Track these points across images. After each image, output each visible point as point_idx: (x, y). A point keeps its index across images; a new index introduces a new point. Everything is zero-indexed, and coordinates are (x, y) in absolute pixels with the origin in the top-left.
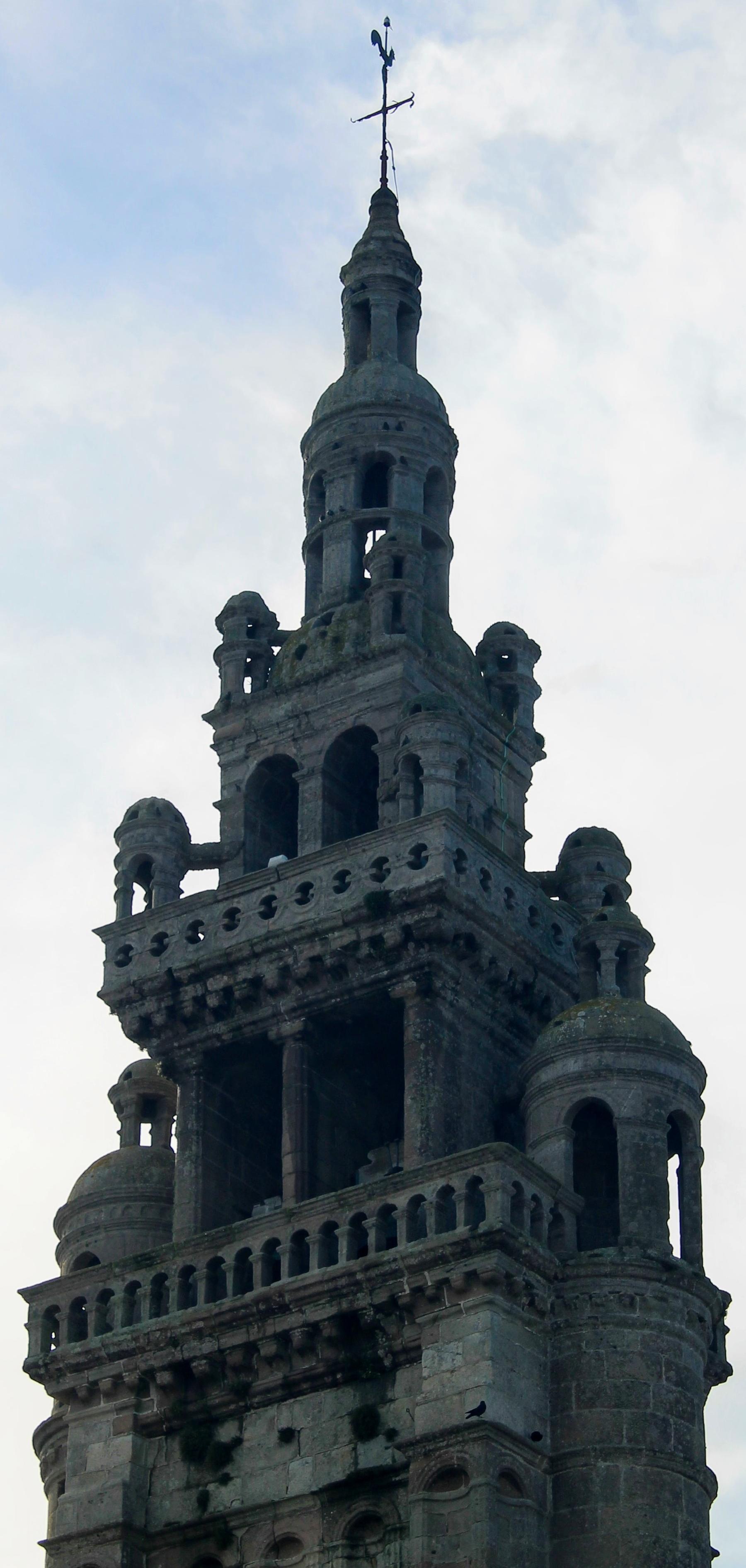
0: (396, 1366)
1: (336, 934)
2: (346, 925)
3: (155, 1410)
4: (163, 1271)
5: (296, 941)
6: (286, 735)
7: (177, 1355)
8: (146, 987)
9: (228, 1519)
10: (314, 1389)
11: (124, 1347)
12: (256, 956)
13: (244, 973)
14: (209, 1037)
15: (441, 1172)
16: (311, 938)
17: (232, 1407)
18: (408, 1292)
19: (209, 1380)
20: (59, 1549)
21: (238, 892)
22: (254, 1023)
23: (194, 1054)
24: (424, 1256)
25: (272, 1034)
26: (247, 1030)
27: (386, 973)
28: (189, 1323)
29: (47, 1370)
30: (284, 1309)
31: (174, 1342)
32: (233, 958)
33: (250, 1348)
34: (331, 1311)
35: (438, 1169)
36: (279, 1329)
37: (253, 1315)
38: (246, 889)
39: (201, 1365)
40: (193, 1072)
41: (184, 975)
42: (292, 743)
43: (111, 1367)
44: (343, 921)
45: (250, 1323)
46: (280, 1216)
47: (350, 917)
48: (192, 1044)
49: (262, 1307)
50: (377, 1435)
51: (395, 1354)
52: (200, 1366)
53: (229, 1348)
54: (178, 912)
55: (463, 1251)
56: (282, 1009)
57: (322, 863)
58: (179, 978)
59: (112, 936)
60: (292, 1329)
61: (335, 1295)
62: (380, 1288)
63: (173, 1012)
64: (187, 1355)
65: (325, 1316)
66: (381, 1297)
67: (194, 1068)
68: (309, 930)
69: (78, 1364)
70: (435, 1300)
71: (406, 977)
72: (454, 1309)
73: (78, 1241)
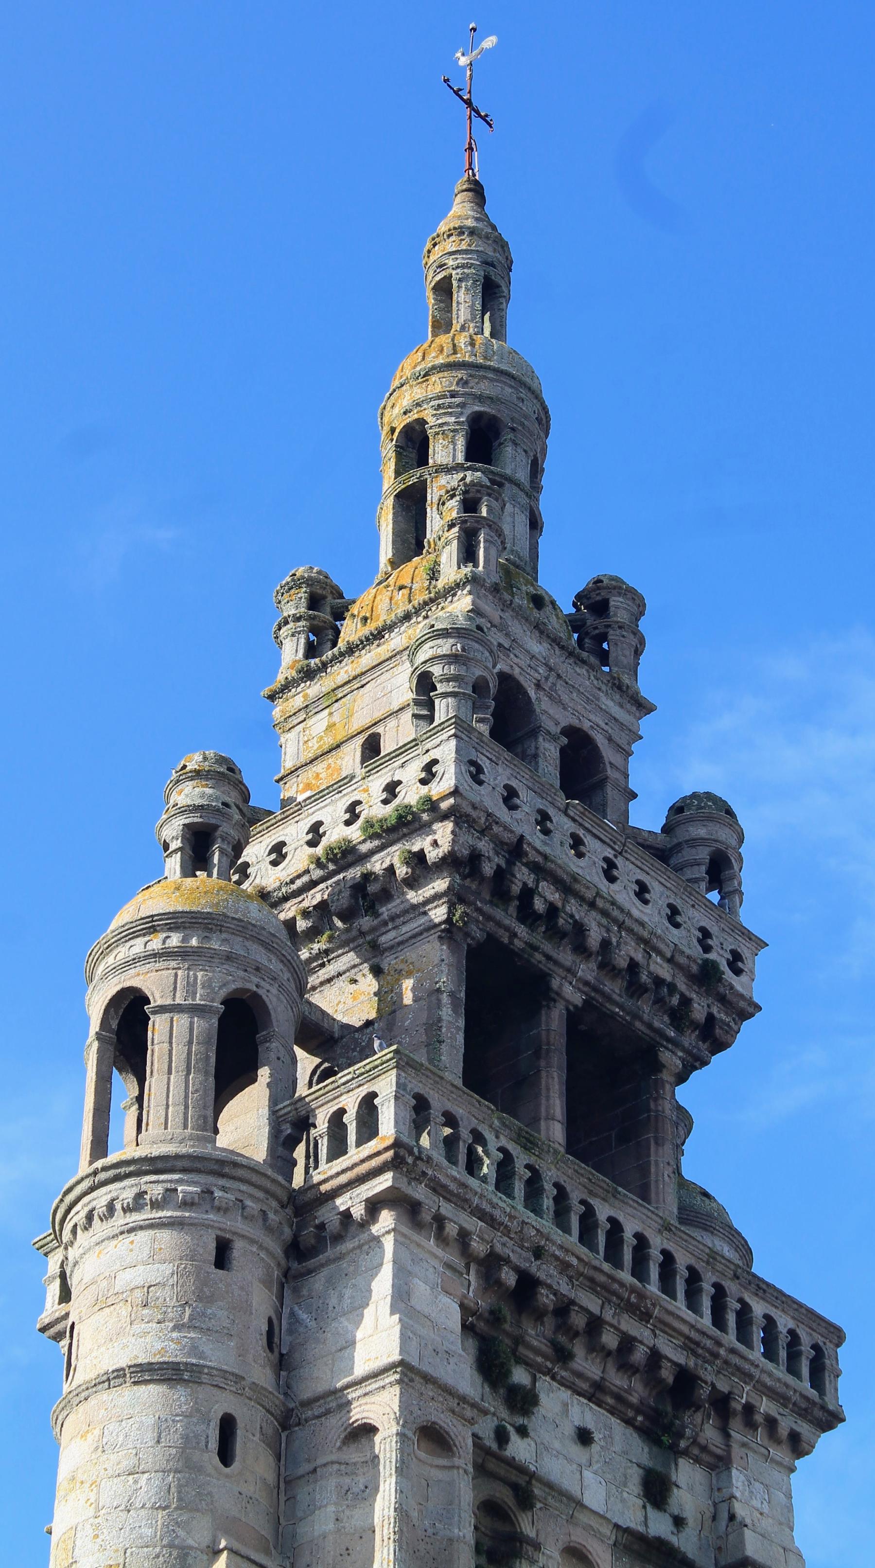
0: (685, 1453)
1: (659, 960)
2: (670, 961)
3: (471, 1294)
4: (537, 1167)
5: (630, 931)
6: (532, 672)
7: (533, 1267)
8: (495, 828)
9: (534, 1482)
10: (612, 1411)
11: (497, 1213)
12: (592, 905)
13: (573, 907)
14: (507, 929)
15: (796, 1315)
16: (640, 940)
17: (539, 1359)
18: (743, 1401)
19: (539, 1315)
20: (412, 1380)
21: (587, 825)
22: (549, 958)
23: (481, 926)
24: (778, 1385)
25: (555, 983)
26: (538, 956)
27: (672, 1034)
28: (567, 1251)
29: (415, 1164)
30: (645, 1317)
31: (538, 1253)
32: (577, 886)
33: (595, 1324)
34: (680, 1358)
35: (796, 1310)
36: (633, 1332)
37: (619, 1297)
38: (594, 831)
39: (547, 1296)
40: (469, 941)
41: (533, 856)
42: (533, 686)
43: (467, 1217)
44: (673, 956)
45: (609, 1302)
46: (660, 1221)
47: (682, 960)
48: (489, 918)
49: (633, 1299)
50: (665, 1511)
51: (695, 1442)
52: (545, 1298)
53: (581, 1307)
54: (530, 784)
55: (806, 1410)
56: (580, 974)
57: (659, 878)
58: (526, 854)
59: (467, 739)
60: (641, 1342)
61: (690, 1345)
62: (725, 1375)
63: (501, 875)
64: (542, 1276)
65: (675, 1359)
66: (723, 1386)
67: (473, 938)
68: (646, 934)
69: (444, 1187)
70: (751, 1425)
71: (680, 1054)
72: (763, 1450)
73: (246, 971)
